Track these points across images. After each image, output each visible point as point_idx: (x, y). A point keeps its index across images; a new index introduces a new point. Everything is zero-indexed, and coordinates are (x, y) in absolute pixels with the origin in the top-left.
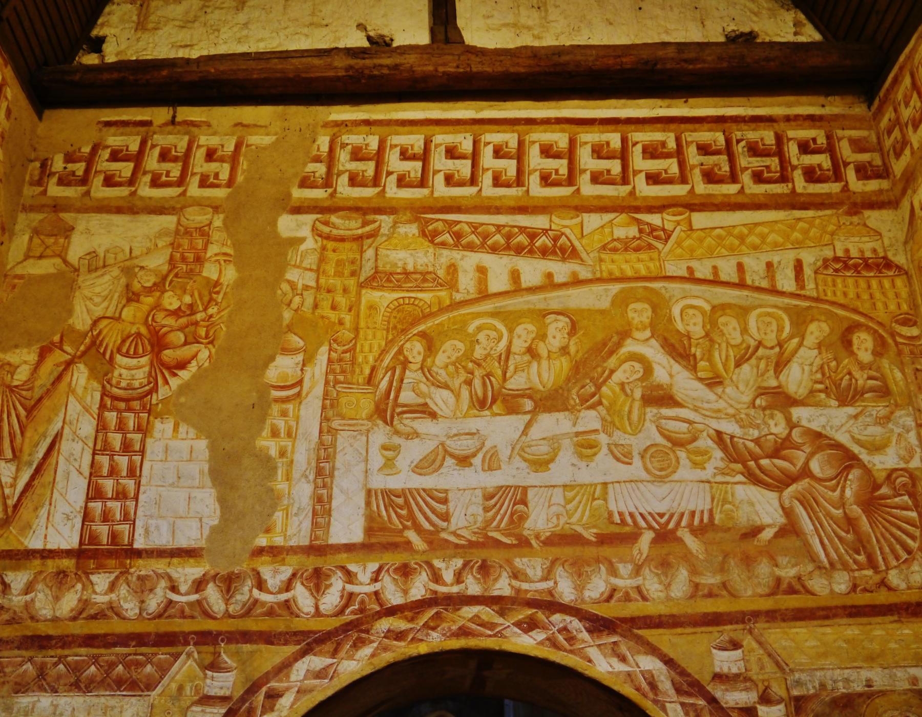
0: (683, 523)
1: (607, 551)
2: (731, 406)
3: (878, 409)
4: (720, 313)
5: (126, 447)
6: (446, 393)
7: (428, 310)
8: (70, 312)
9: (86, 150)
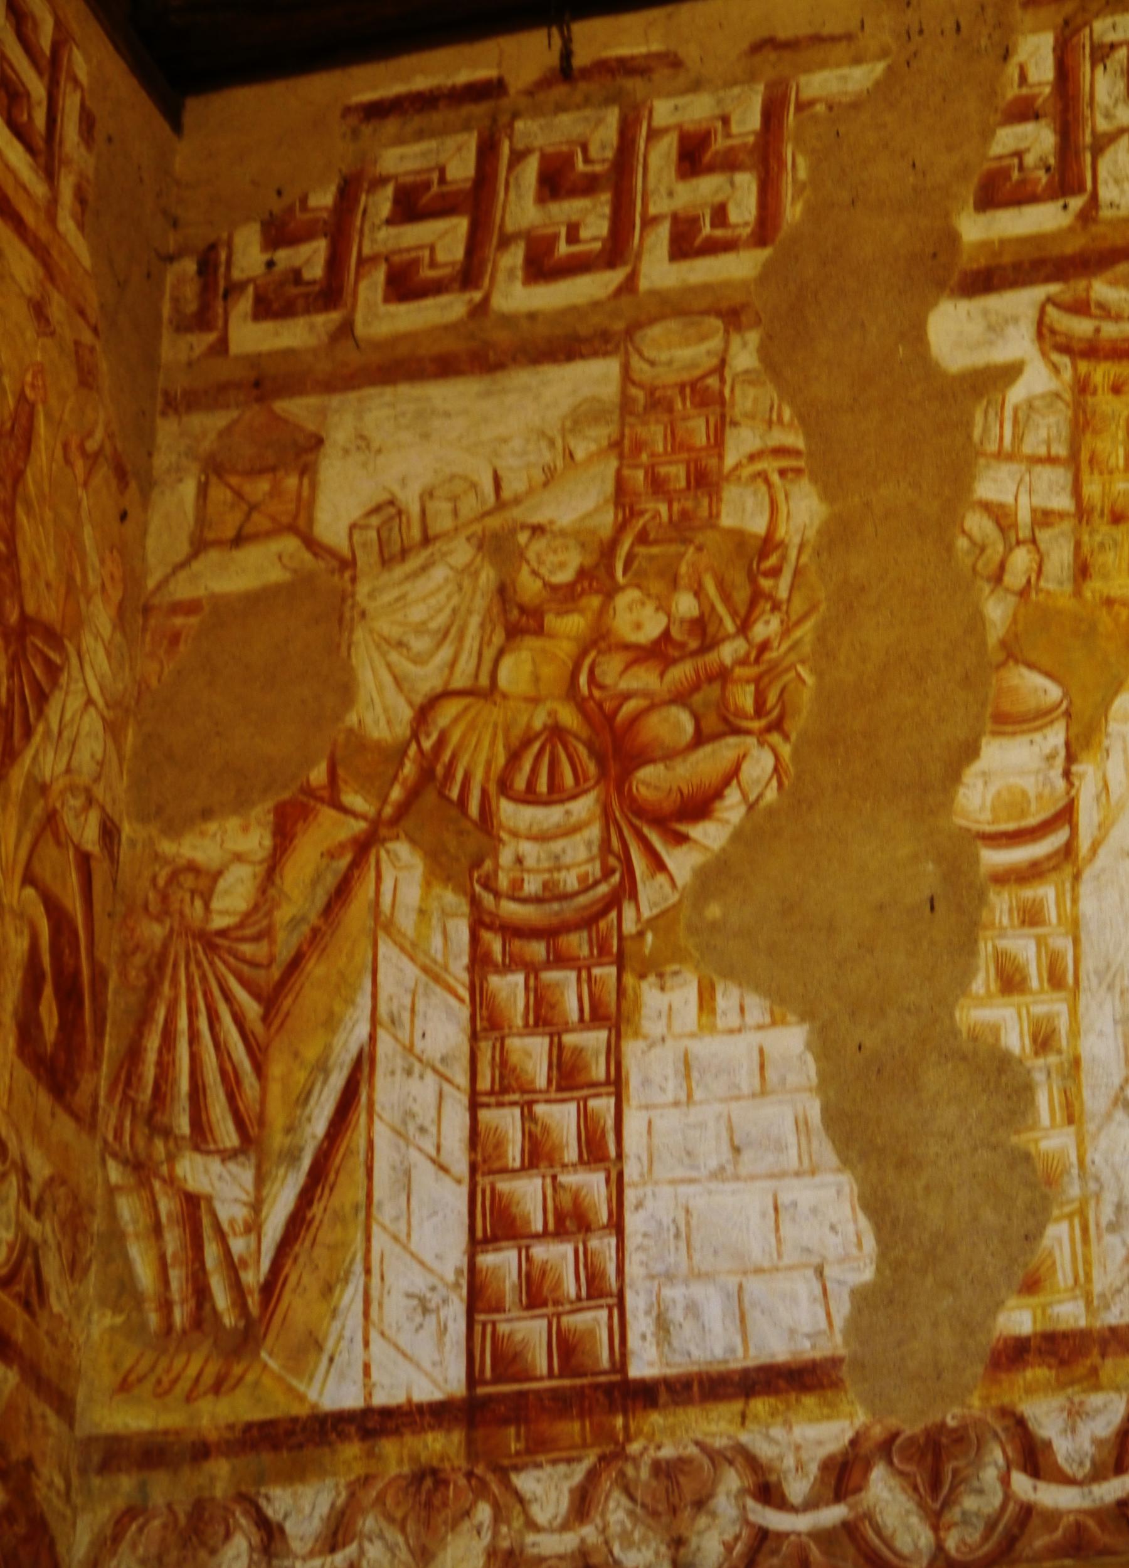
5: (567, 1075)
8: (347, 692)
9: (324, 199)
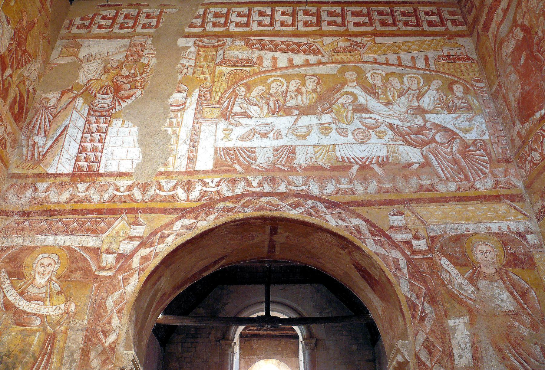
0: (373, 162)
1: (336, 173)
5: (99, 131)
6: (255, 107)
8: (77, 77)
9: (91, 15)
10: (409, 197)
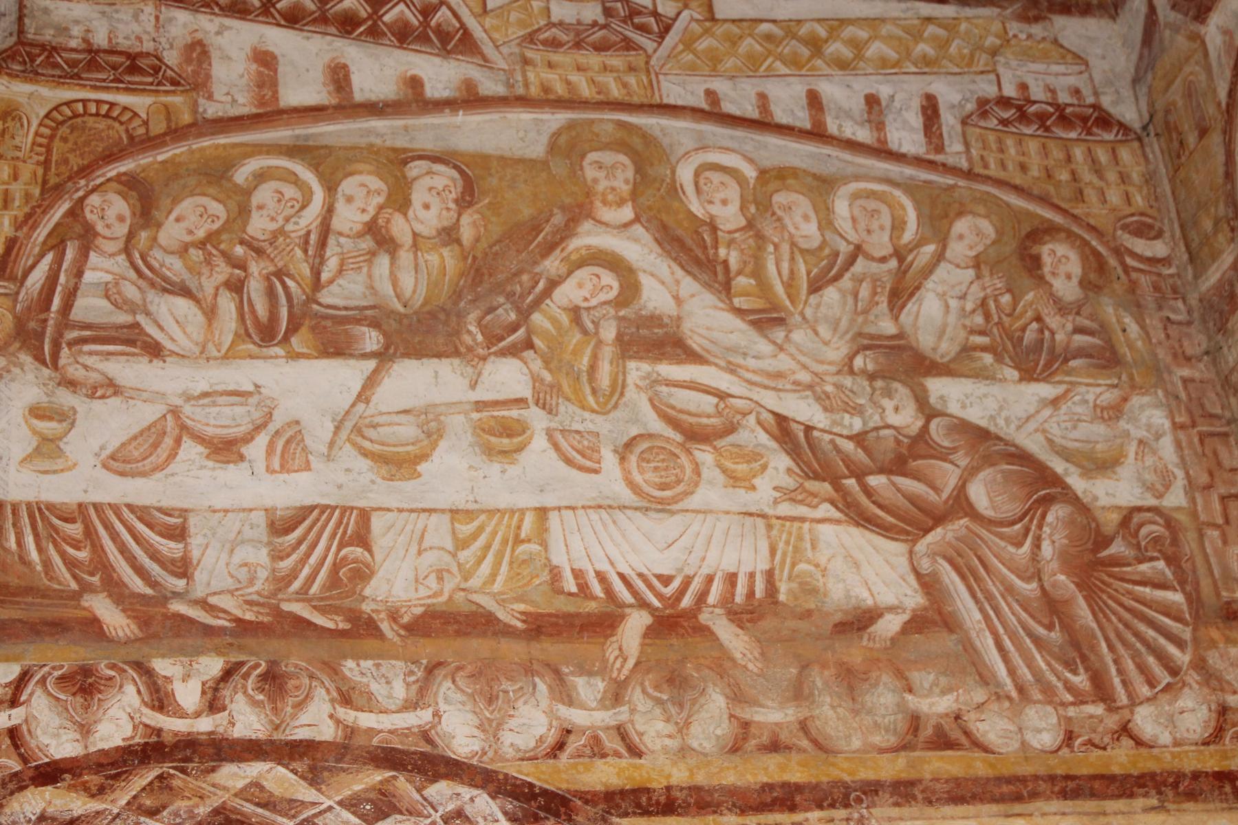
0: (712, 599)
1: (549, 649)
2: (804, 367)
3: (1098, 390)
4: (772, 186)
7: (142, 131)
10: (866, 774)
